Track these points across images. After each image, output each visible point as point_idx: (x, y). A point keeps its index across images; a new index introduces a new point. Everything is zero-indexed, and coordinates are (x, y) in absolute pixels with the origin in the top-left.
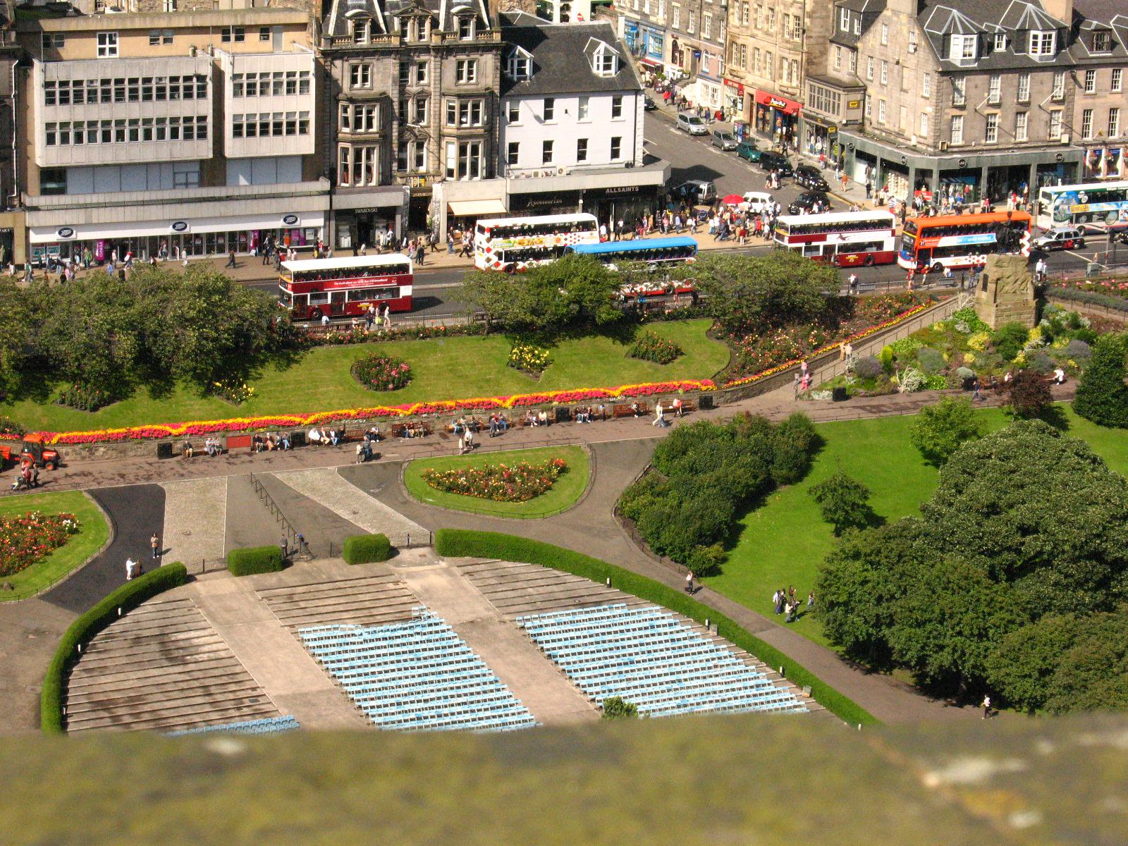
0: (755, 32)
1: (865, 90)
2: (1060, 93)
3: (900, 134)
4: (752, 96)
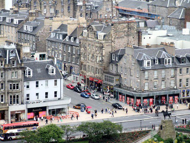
0: (88, 61)
1: (120, 76)
2: (173, 74)
3: (131, 88)
4: (88, 79)
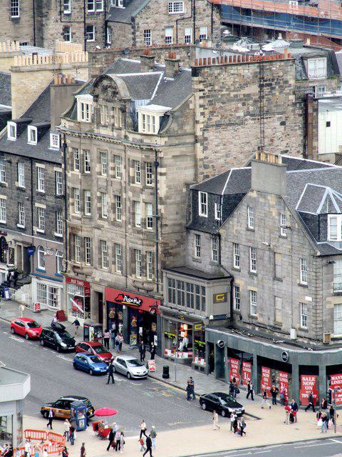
0: (100, 222)
1: (232, 281)
3: (276, 328)
4: (100, 295)
